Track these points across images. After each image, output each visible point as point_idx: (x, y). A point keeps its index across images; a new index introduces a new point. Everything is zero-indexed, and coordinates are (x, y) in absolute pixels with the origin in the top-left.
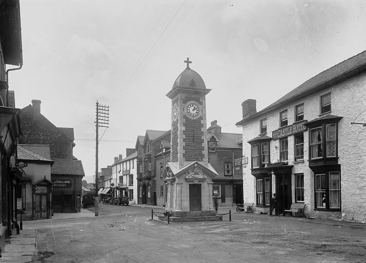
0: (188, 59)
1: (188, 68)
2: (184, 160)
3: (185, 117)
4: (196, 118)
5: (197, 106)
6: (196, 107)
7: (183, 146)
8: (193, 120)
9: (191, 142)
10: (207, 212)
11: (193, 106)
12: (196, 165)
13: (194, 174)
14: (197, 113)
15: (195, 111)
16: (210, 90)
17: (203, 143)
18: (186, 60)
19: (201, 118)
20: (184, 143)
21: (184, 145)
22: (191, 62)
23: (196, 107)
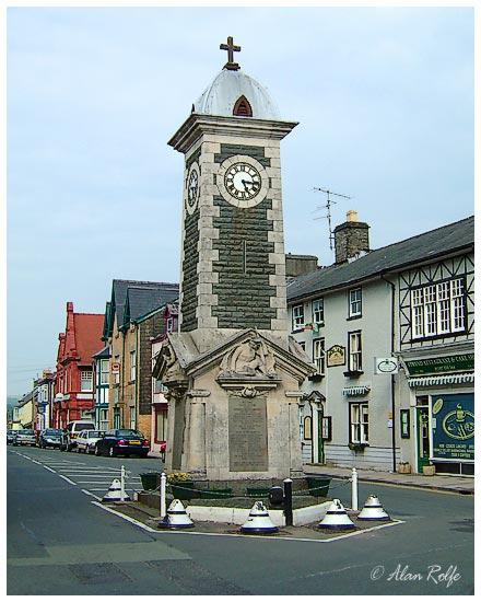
0: (230, 40)
3: (219, 200)
4: (252, 203)
5: (255, 170)
16: (293, 125)
19: (267, 204)
22: (238, 49)
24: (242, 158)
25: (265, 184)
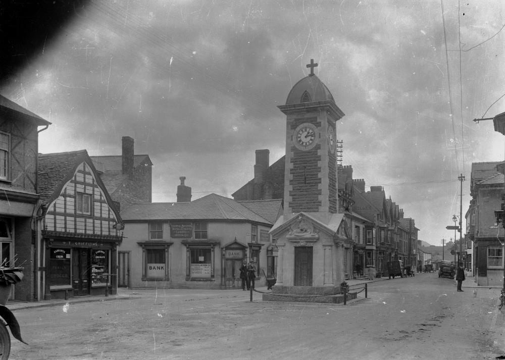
0: (312, 61)
1: (312, 75)
2: (291, 211)
6: (311, 131)
7: (290, 192)
8: (305, 152)
9: (302, 183)
10: (318, 288)
11: (306, 131)
12: (300, 218)
13: (299, 230)
14: (311, 140)
15: (309, 138)
17: (319, 185)
18: (315, 63)
20: (291, 186)
21: (292, 190)
23: (311, 131)
24: (306, 124)
25: (317, 135)
